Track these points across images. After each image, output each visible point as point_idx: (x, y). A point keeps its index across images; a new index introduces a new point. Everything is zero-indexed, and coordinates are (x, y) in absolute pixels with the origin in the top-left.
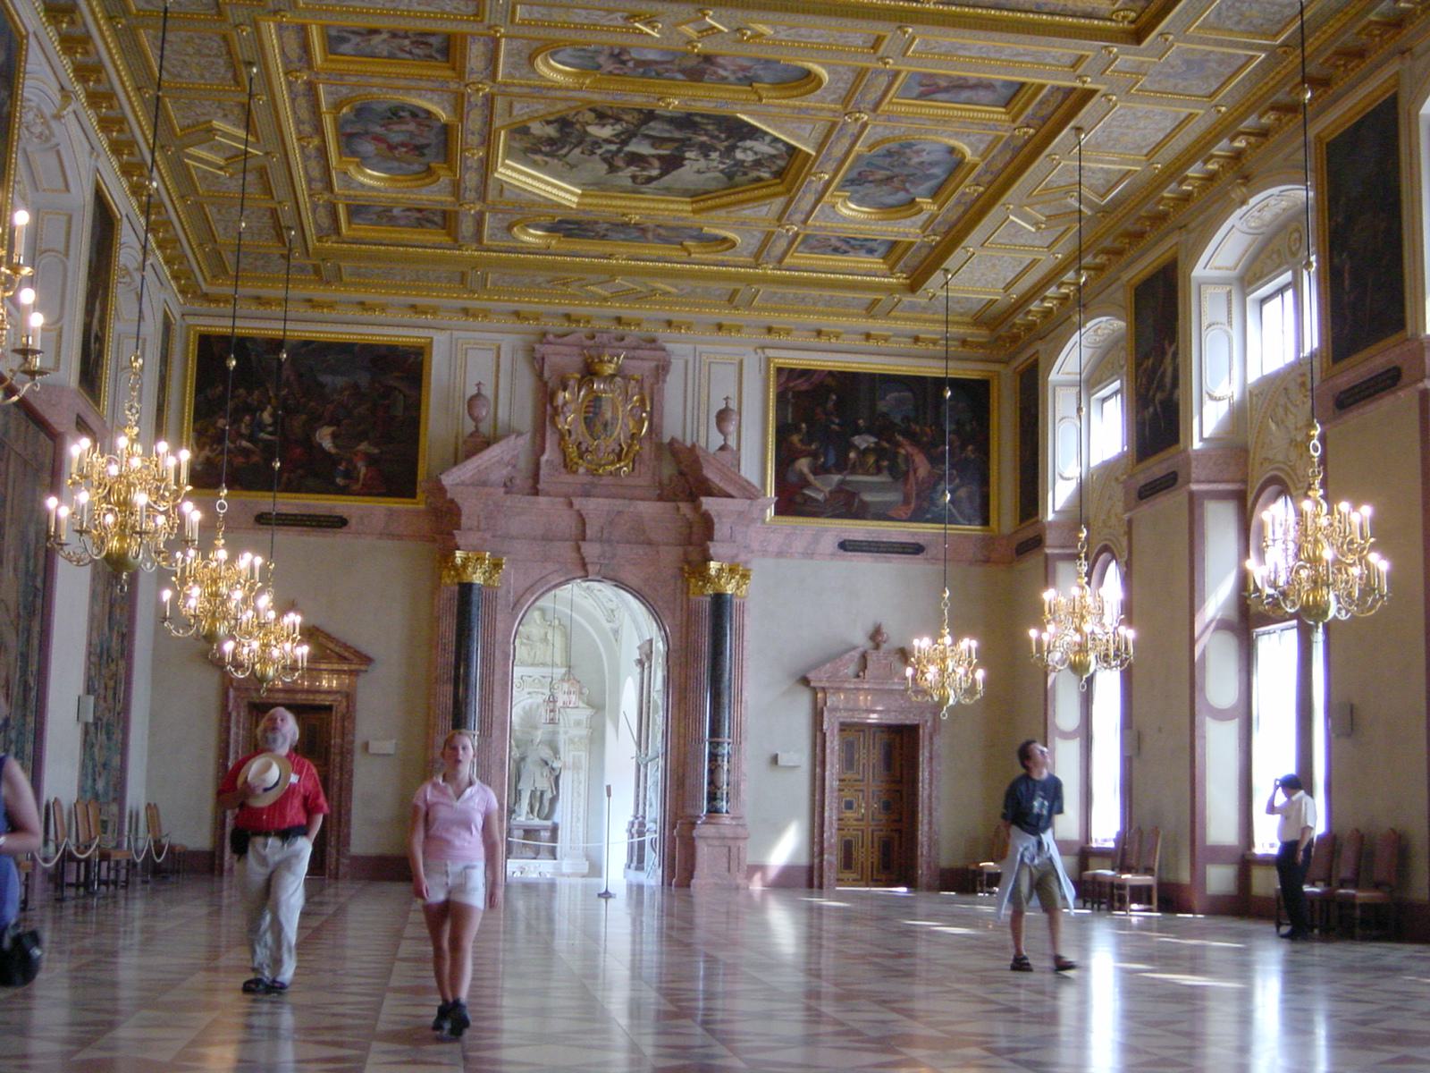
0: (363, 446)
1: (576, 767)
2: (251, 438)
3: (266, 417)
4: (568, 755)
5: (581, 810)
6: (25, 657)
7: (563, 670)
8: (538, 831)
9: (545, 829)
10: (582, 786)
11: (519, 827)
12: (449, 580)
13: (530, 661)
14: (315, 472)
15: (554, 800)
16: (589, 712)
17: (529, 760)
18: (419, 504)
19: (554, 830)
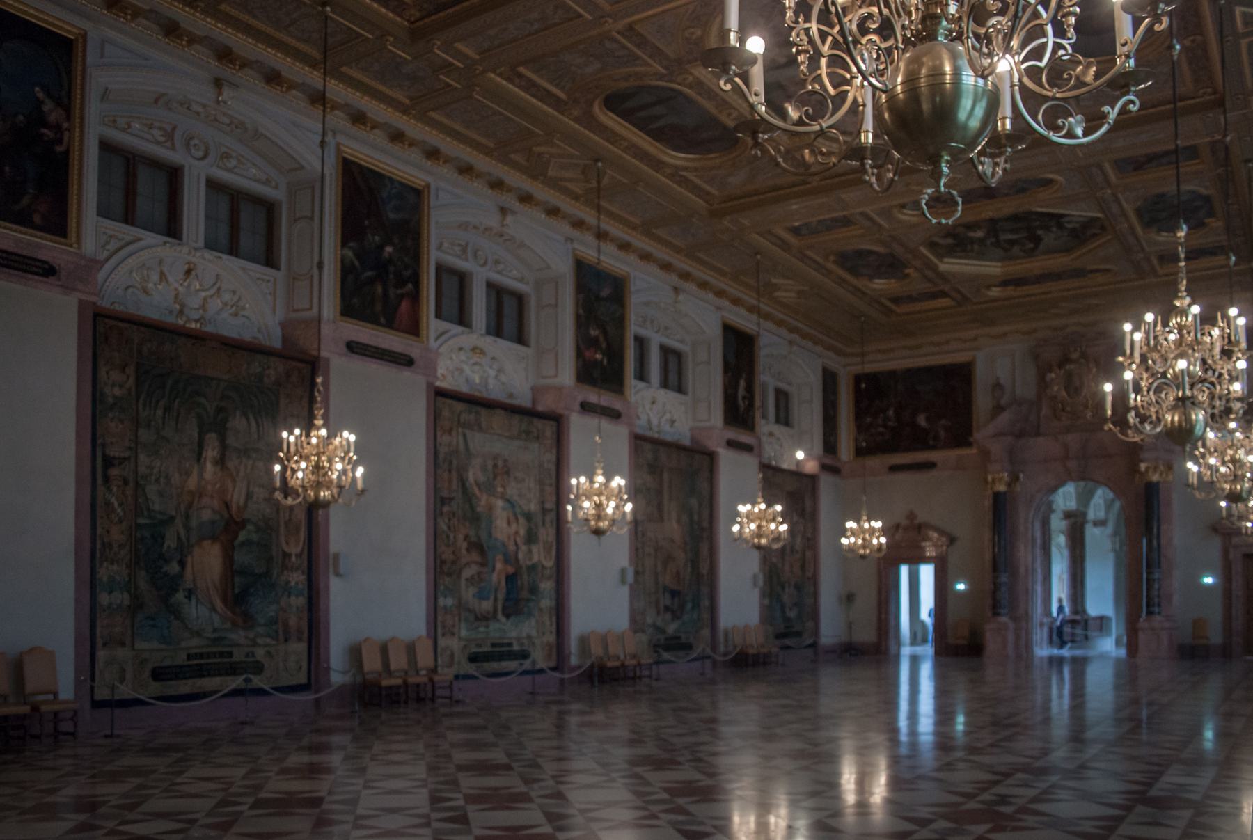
0: (943, 422)
2: (885, 426)
3: (891, 413)
6: (695, 563)
12: (989, 493)
14: (922, 440)
18: (974, 451)
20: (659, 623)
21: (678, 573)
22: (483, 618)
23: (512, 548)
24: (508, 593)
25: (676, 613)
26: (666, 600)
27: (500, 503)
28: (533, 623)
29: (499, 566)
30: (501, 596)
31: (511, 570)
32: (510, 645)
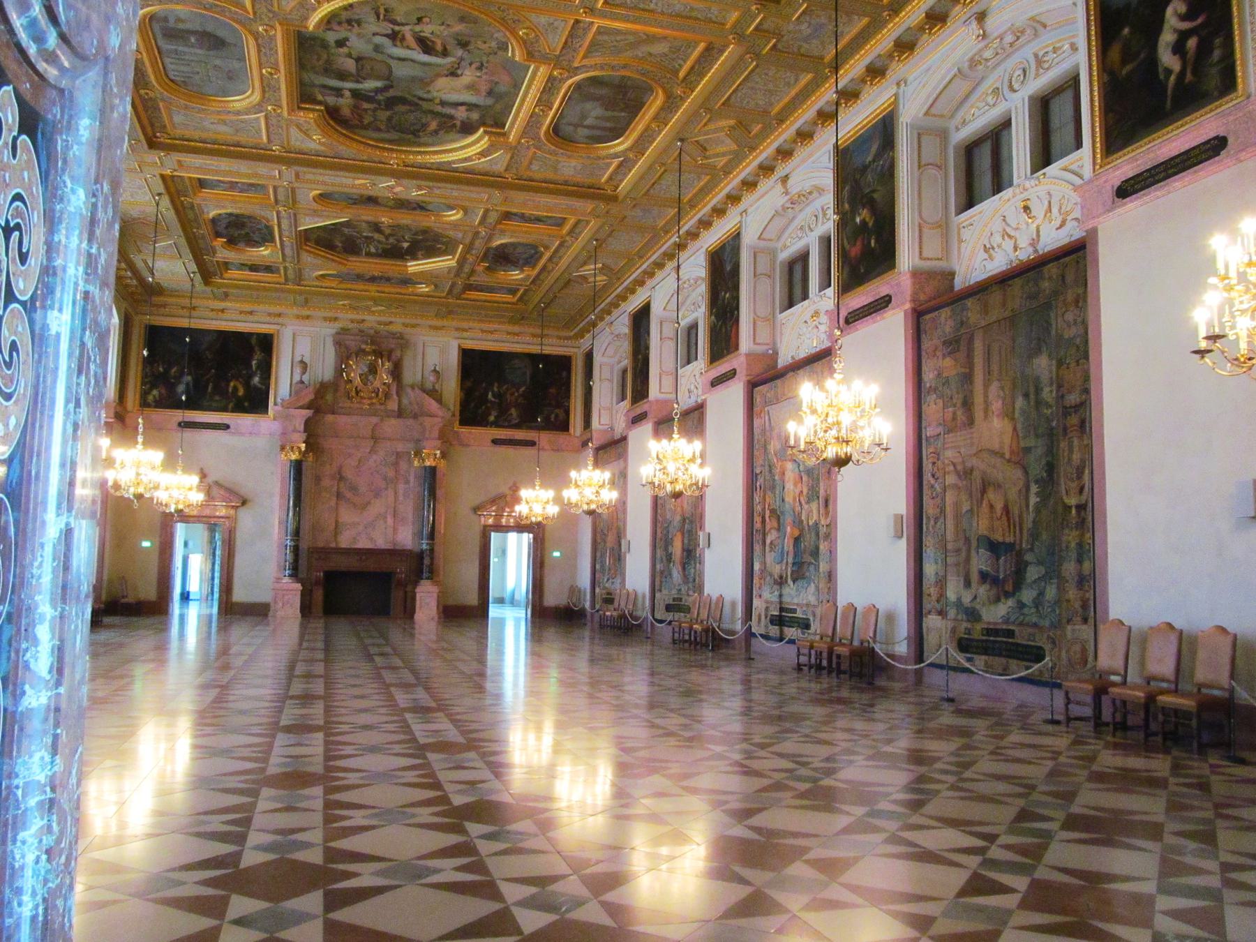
20: (967, 600)
21: (1006, 509)
22: (781, 582)
23: (798, 509)
24: (795, 558)
25: (1004, 584)
26: (980, 561)
27: (790, 466)
28: (812, 587)
29: (789, 529)
30: (790, 560)
31: (797, 533)
32: (794, 611)
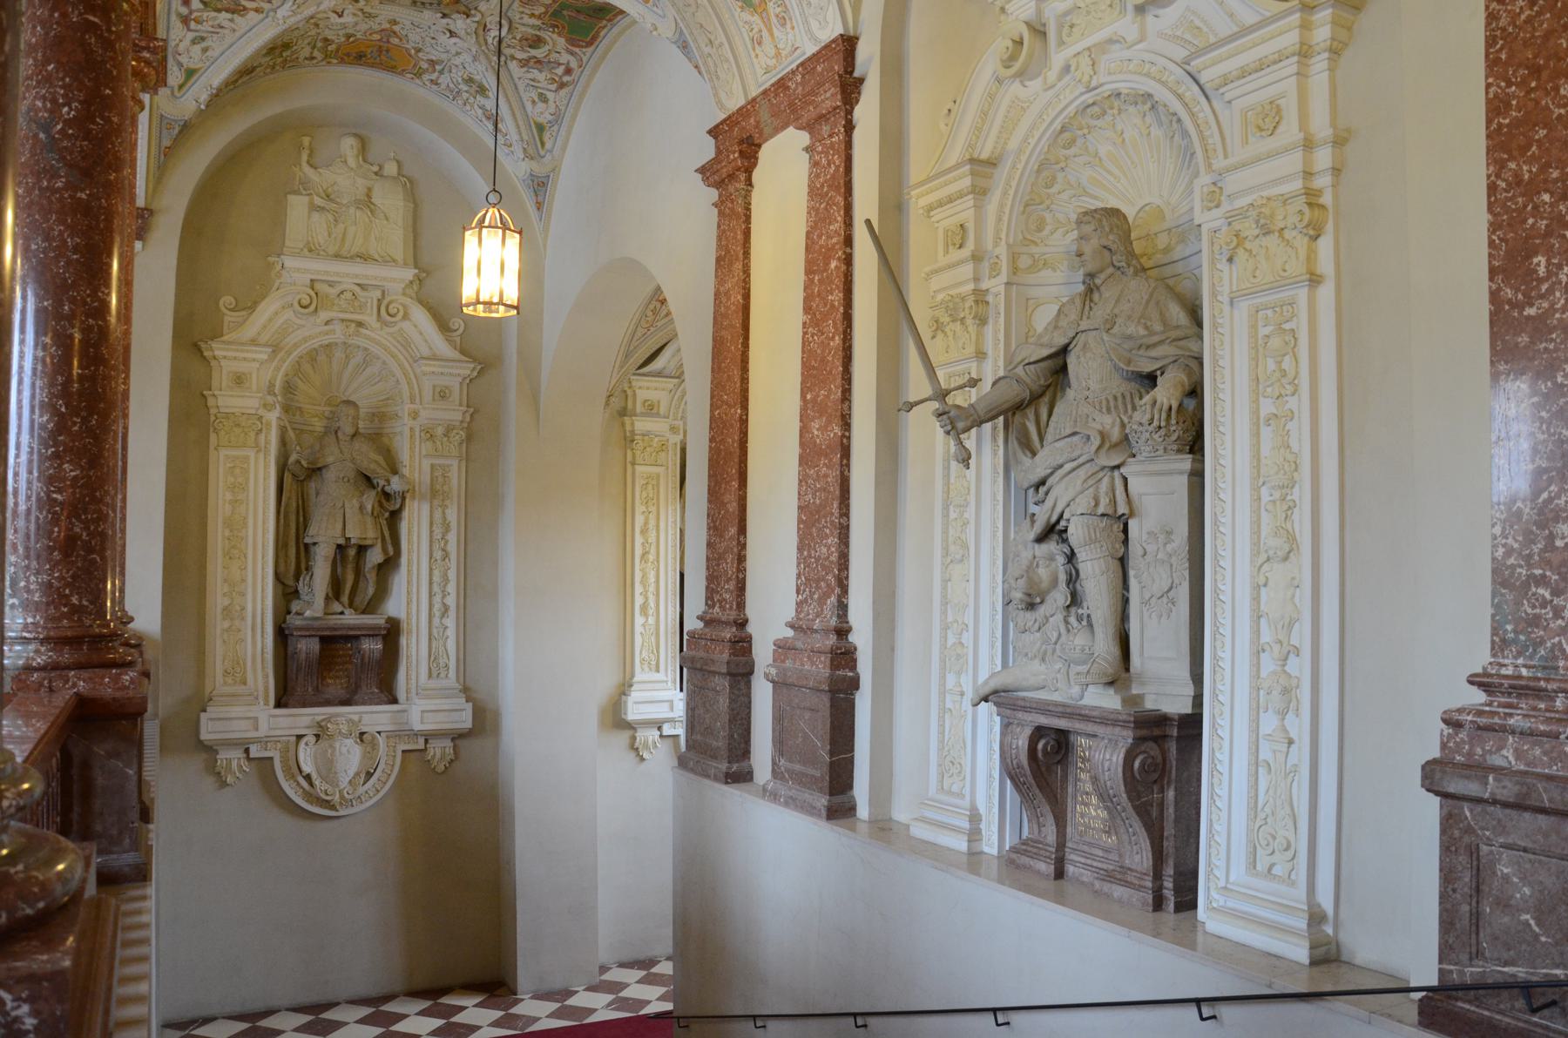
1: (436, 493)
4: (416, 462)
5: (451, 588)
7: (409, 274)
8: (357, 637)
9: (372, 633)
10: (452, 537)
11: (308, 631)
13: (332, 250)
15: (389, 564)
16: (466, 369)
17: (330, 475)
19: (391, 633)
